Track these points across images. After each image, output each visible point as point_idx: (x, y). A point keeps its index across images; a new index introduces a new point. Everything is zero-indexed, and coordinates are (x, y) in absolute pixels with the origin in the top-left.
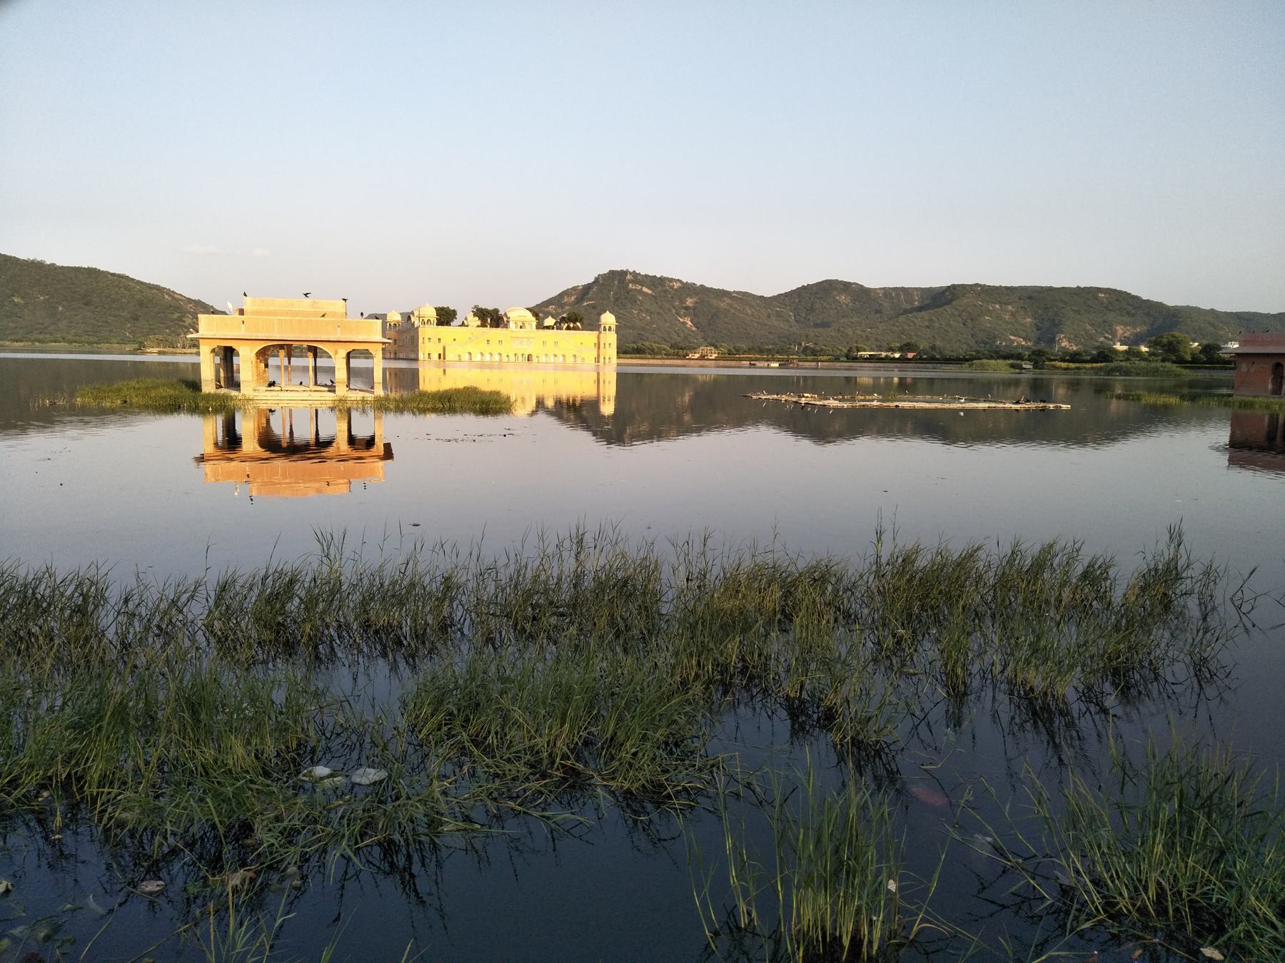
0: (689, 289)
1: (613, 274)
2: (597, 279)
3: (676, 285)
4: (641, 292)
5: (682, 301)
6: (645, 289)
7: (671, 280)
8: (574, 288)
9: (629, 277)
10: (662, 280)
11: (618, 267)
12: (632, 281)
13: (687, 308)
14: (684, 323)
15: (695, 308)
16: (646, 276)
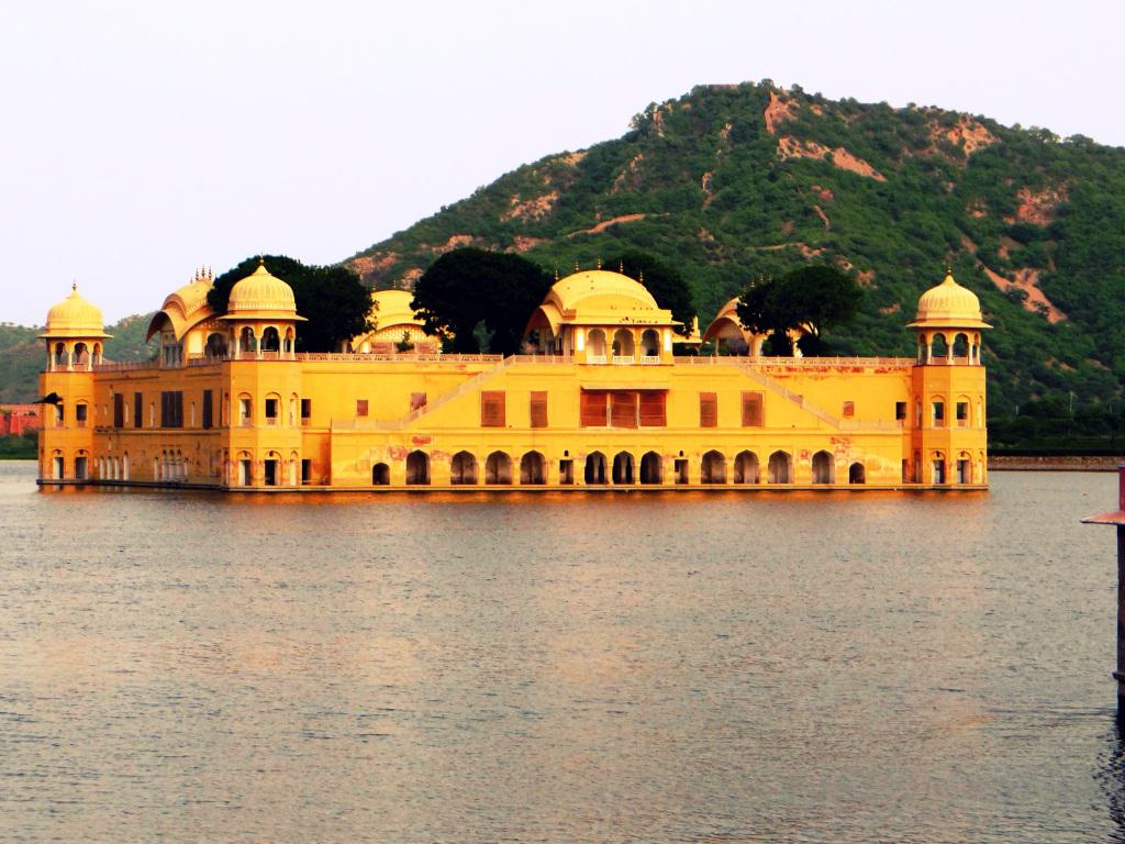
0: (1024, 154)
1: (708, 104)
2: (644, 126)
3: (973, 141)
4: (826, 169)
5: (1002, 207)
6: (844, 160)
7: (951, 120)
8: (551, 167)
9: (775, 111)
10: (915, 120)
11: (729, 75)
12: (786, 129)
13: (1022, 234)
14: (1017, 297)
15: (1055, 233)
16: (849, 106)
